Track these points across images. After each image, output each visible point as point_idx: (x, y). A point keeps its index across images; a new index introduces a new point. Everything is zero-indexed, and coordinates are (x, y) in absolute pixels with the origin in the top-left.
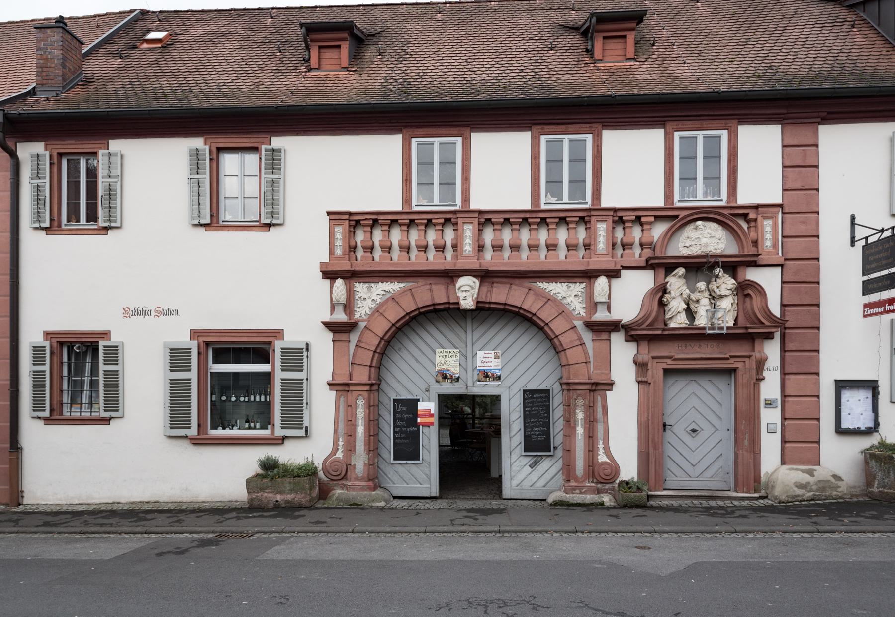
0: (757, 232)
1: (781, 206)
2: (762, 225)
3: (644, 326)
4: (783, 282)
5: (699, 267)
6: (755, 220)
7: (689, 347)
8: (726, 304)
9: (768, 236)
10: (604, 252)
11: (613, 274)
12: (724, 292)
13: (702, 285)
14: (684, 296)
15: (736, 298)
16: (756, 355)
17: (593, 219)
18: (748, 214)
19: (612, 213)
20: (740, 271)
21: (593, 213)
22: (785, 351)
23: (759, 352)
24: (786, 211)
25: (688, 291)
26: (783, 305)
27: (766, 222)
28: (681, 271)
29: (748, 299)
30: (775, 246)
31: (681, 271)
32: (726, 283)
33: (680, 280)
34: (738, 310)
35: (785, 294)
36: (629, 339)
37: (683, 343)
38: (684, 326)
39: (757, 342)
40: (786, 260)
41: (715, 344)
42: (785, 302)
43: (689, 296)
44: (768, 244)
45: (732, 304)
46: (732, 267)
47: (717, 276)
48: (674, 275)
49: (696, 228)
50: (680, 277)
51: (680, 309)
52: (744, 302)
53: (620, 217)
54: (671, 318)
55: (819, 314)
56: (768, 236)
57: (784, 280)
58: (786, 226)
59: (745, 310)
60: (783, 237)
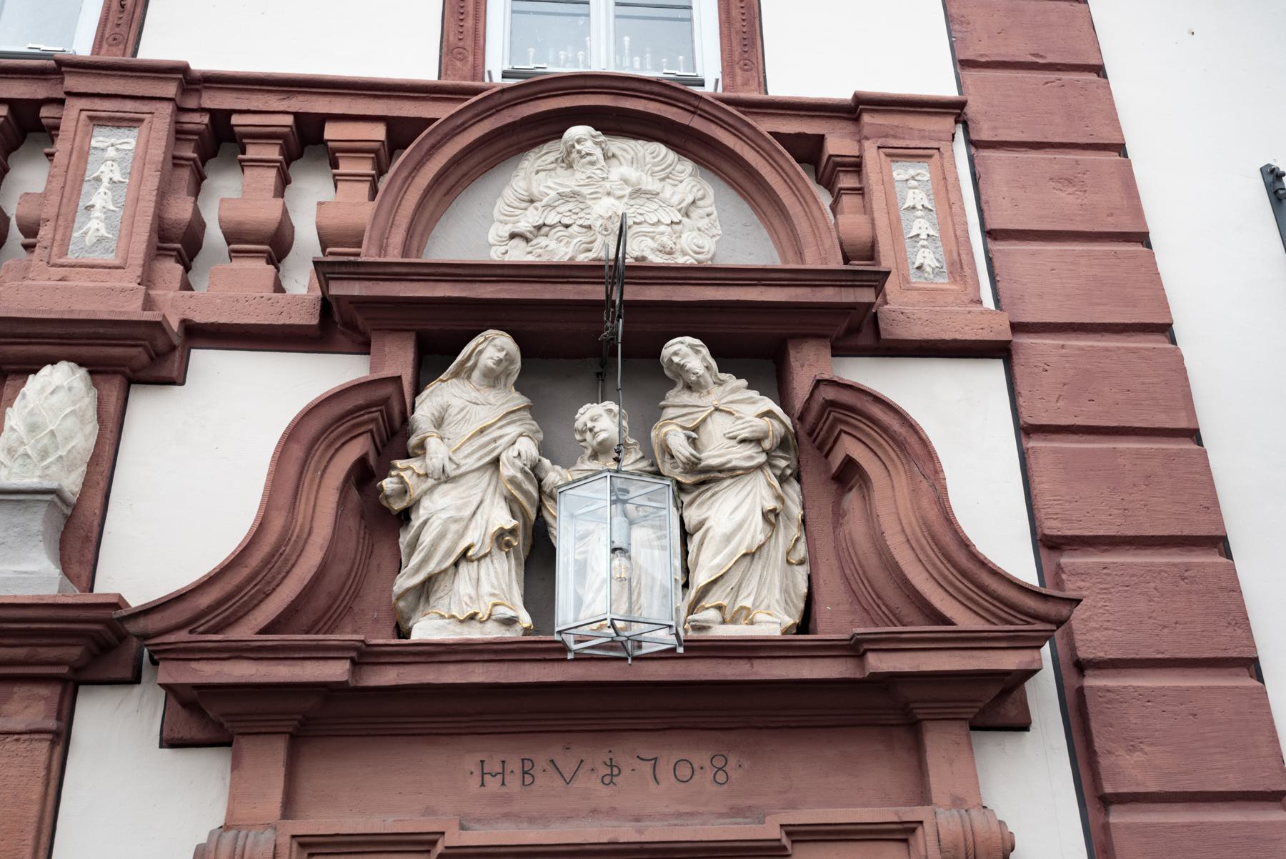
0: (867, 210)
1: (954, 109)
2: (888, 183)
3: (245, 632)
4: (1025, 431)
5: (589, 336)
6: (856, 166)
7: (546, 781)
8: (734, 514)
9: (921, 226)
10: (110, 258)
11: (132, 358)
12: (717, 451)
13: (601, 418)
14: (507, 470)
15: (793, 490)
16: (941, 820)
17: (72, 114)
18: (820, 139)
19: (170, 90)
20: (810, 366)
21: (73, 83)
22: (1107, 801)
23: (957, 802)
24: (985, 136)
25: (528, 447)
26: (1047, 544)
27: (901, 172)
28: (495, 346)
29: (852, 500)
30: (958, 266)
31: (495, 346)
32: (728, 414)
33: (491, 395)
34: (811, 560)
35: (1042, 485)
36: (191, 730)
37: (503, 755)
38: (492, 632)
39: (940, 745)
40: (1017, 327)
41: (700, 758)
42: (1053, 527)
43: (535, 472)
44: (928, 257)
45: (771, 518)
46: (754, 339)
47: (680, 379)
48: (464, 373)
49: (567, 162)
50: (493, 378)
51: (477, 536)
52: (838, 515)
53: (220, 118)
54: (425, 589)
55: (1234, 588)
56: (921, 226)
57: (1027, 419)
58: (998, 189)
59: (844, 554)
60: (990, 234)
